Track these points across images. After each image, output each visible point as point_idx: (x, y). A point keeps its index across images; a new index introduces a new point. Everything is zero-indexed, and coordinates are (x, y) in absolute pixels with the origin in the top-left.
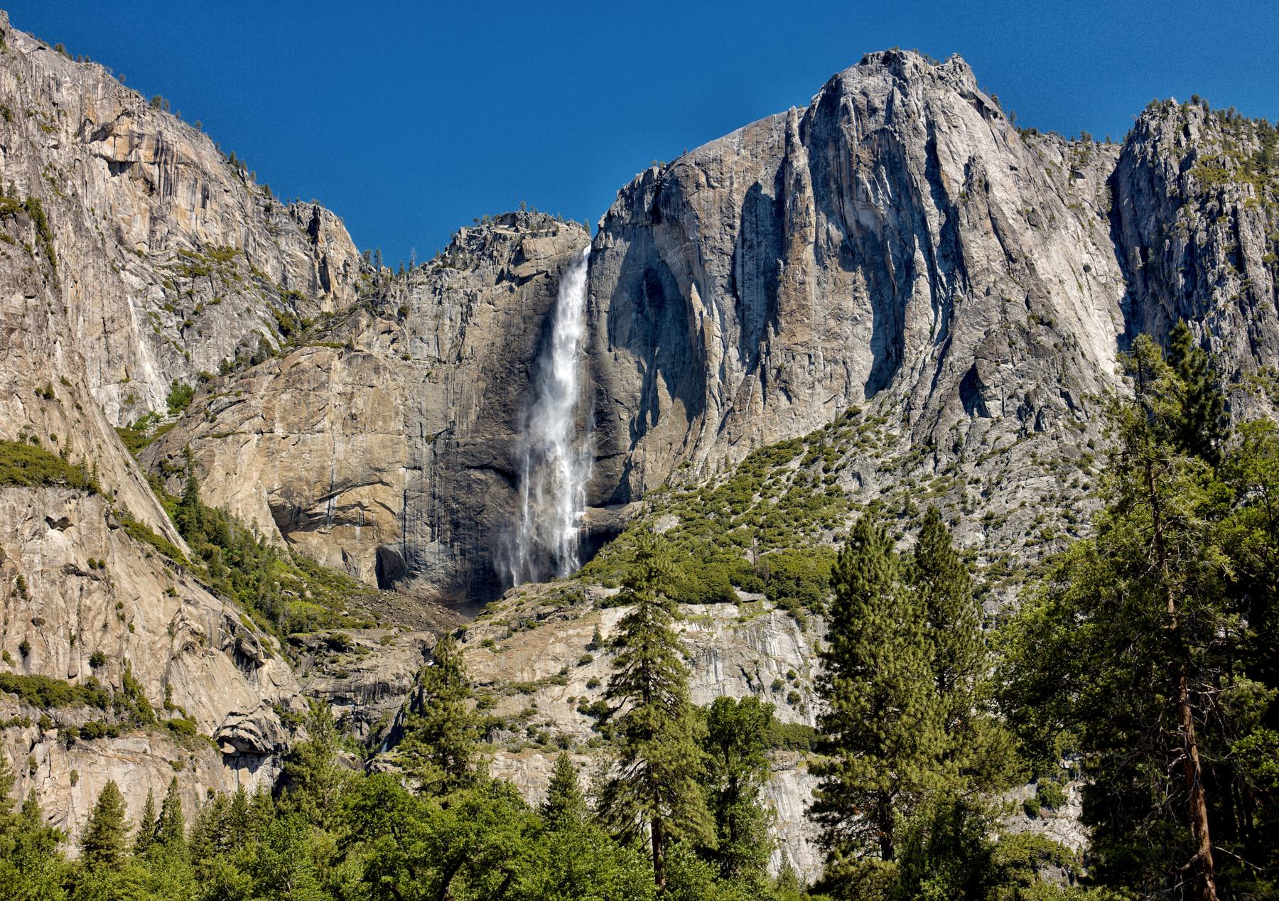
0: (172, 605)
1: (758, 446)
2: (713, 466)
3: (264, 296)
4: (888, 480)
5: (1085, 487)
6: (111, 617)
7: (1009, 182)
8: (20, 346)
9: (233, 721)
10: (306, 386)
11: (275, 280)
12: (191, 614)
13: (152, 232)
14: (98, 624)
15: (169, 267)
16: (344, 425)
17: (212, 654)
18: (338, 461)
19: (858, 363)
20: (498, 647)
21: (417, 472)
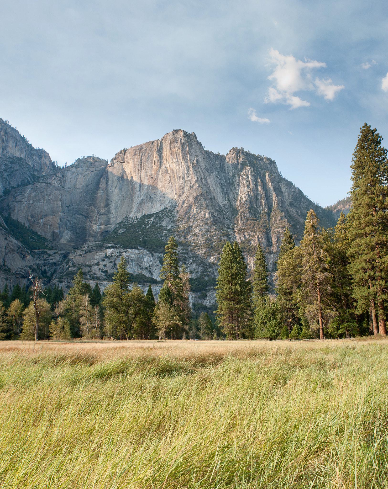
0: (6, 242)
1: (144, 214)
2: (133, 218)
3: (28, 170)
7: (203, 161)
9: (19, 270)
10: (38, 192)
11: (32, 166)
12: (10, 244)
13: (3, 152)
15: (6, 161)
16: (47, 202)
18: (45, 210)
20: (83, 256)
21: (64, 214)
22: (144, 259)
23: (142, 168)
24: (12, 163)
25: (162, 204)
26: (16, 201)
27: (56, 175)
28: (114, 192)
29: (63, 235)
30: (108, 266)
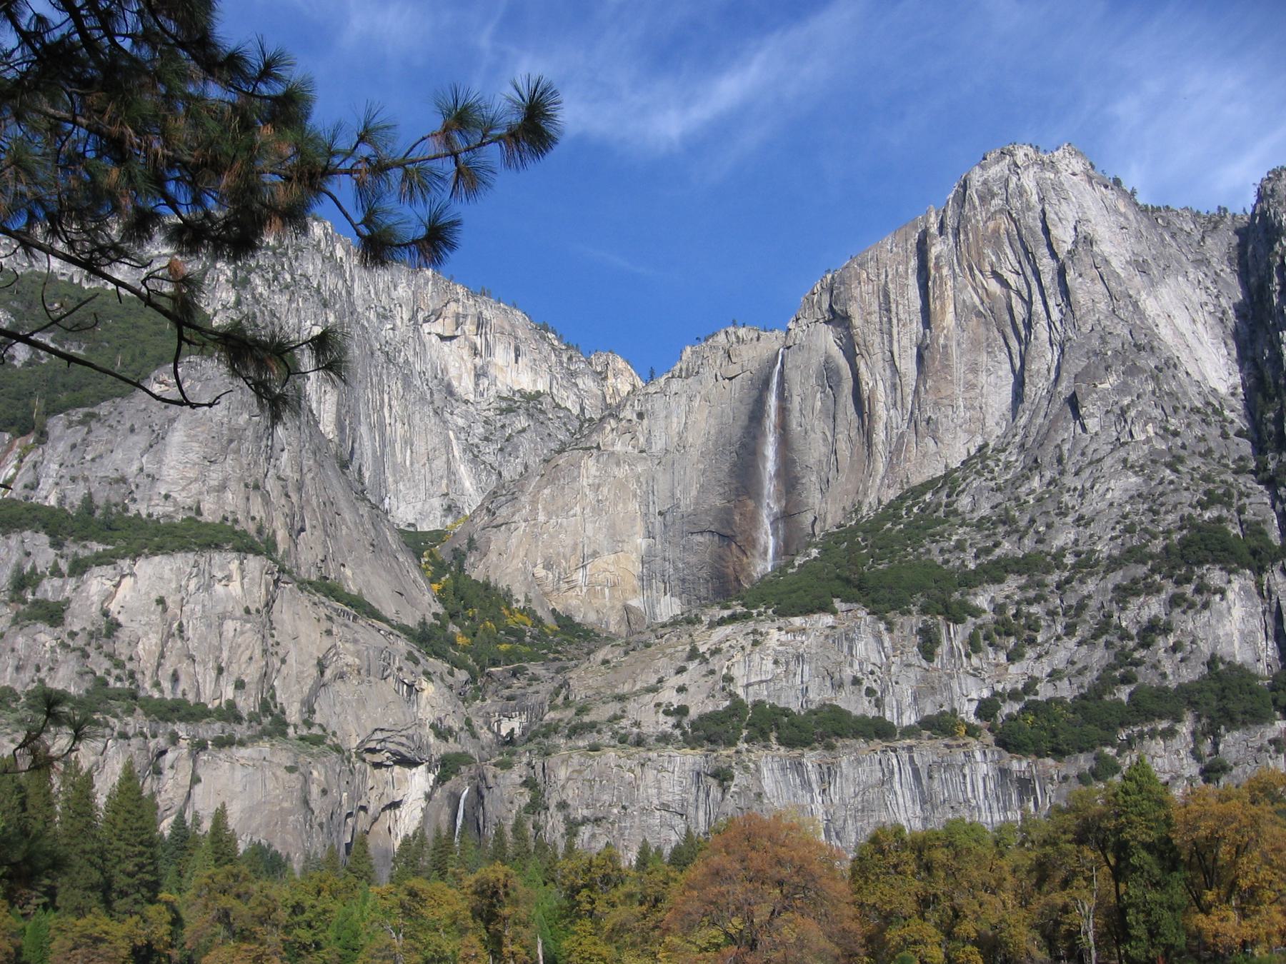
0: (327, 642)
1: (906, 487)
3: (565, 424)
4: (999, 497)
5: (1171, 482)
6: (257, 651)
8: (238, 451)
9: (379, 735)
11: (576, 411)
12: (347, 650)
13: (477, 385)
14: (245, 657)
16: (593, 510)
17: (370, 682)
18: (588, 538)
19: (992, 406)
22: (851, 648)
23: (895, 321)
24: (502, 411)
25: (972, 434)
26: (495, 523)
27: (616, 417)
28: (810, 432)
29: (657, 611)
30: (692, 689)
